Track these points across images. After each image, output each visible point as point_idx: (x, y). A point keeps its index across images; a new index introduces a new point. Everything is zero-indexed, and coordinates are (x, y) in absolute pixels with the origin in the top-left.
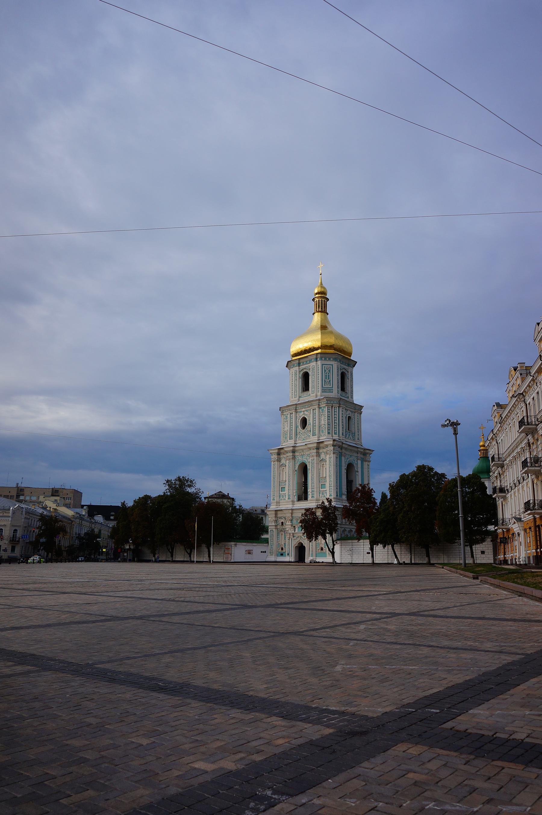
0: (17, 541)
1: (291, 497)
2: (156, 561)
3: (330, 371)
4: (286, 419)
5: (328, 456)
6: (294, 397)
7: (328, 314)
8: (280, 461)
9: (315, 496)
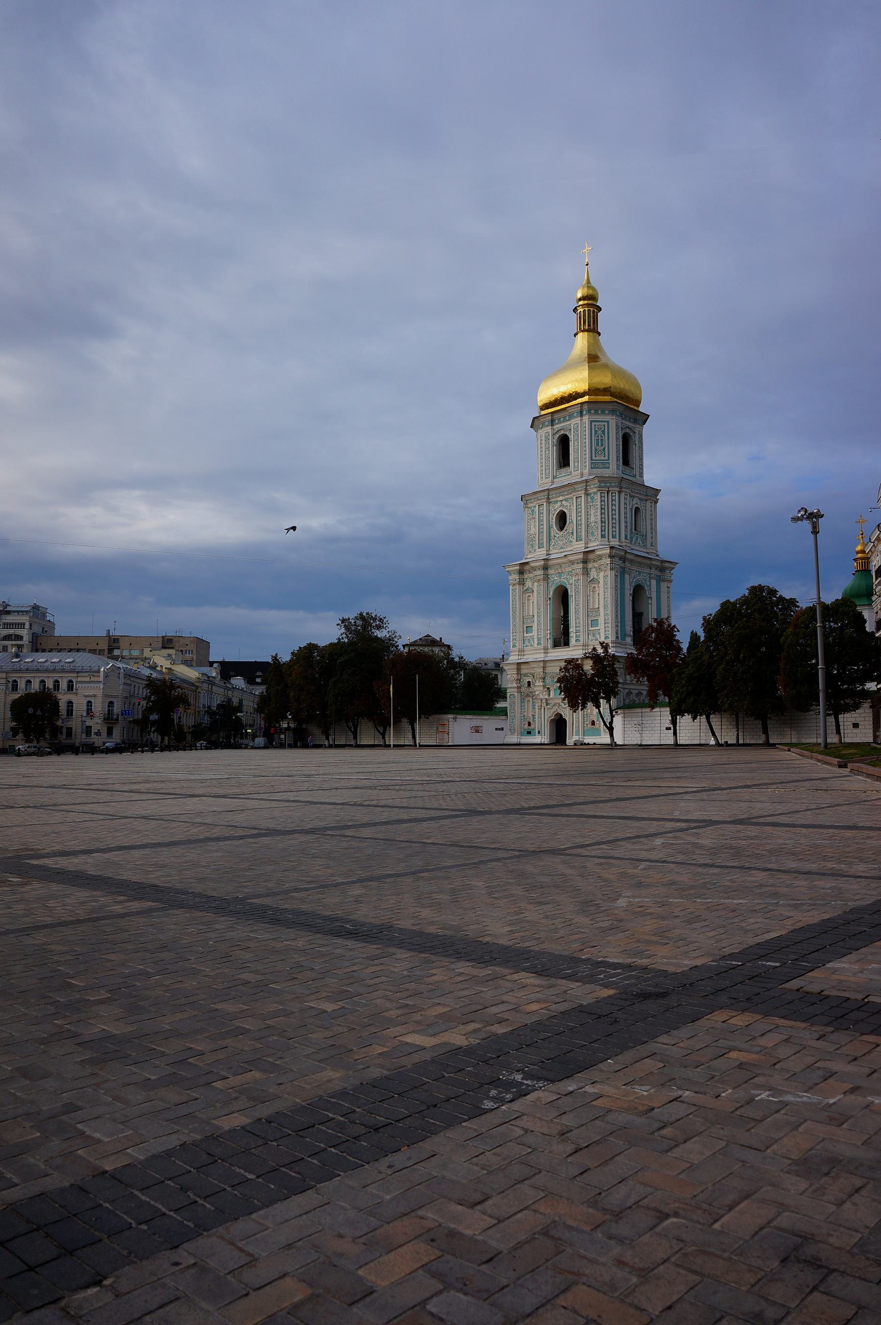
0: (116, 720)
1: (542, 642)
2: (330, 746)
3: (603, 432)
4: (532, 515)
5: (602, 574)
6: (544, 478)
7: (599, 334)
8: (524, 584)
9: (581, 639)
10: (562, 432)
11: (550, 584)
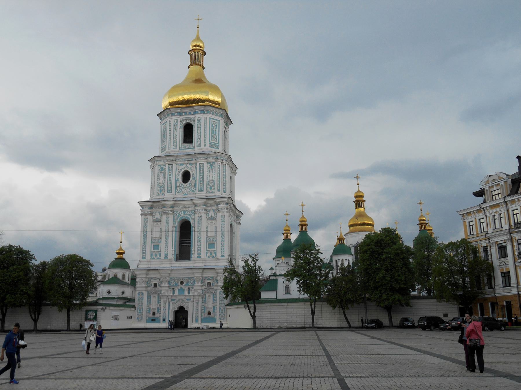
3: (216, 126)
4: (162, 170)
5: (219, 215)
8: (153, 216)
9: (202, 256)
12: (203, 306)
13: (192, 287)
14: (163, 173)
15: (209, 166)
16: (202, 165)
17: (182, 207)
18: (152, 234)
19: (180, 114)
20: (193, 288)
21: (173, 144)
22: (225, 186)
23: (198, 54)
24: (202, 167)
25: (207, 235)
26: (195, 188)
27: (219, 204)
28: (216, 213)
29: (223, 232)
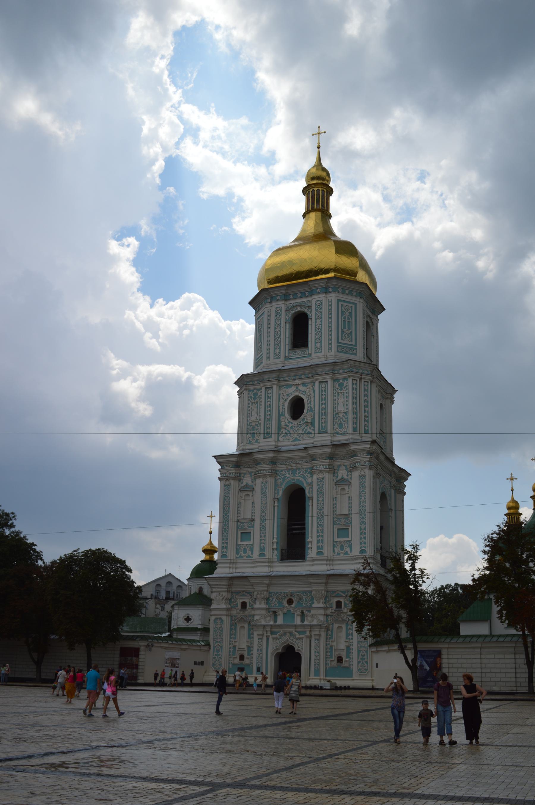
1: (266, 553)
3: (351, 313)
4: (255, 399)
5: (356, 475)
8: (240, 480)
9: (325, 551)
10: (299, 309)
11: (279, 481)
12: (328, 646)
13: (307, 609)
14: (257, 402)
15: (337, 386)
16: (323, 386)
17: (290, 463)
18: (239, 512)
19: (286, 297)
20: (309, 611)
21: (275, 351)
22: (368, 421)
23: (319, 193)
24: (324, 389)
25: (335, 512)
26: (312, 428)
27: (355, 455)
28: (351, 472)
29: (363, 506)
